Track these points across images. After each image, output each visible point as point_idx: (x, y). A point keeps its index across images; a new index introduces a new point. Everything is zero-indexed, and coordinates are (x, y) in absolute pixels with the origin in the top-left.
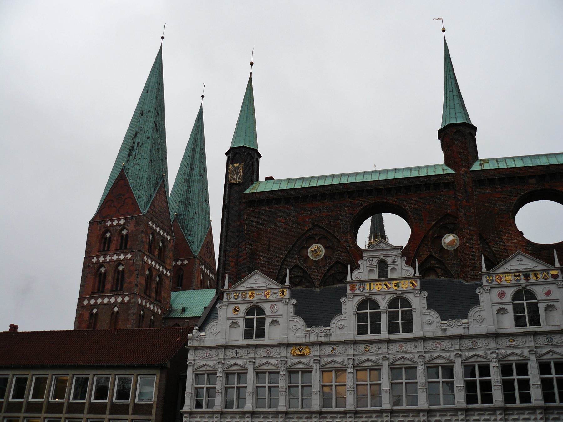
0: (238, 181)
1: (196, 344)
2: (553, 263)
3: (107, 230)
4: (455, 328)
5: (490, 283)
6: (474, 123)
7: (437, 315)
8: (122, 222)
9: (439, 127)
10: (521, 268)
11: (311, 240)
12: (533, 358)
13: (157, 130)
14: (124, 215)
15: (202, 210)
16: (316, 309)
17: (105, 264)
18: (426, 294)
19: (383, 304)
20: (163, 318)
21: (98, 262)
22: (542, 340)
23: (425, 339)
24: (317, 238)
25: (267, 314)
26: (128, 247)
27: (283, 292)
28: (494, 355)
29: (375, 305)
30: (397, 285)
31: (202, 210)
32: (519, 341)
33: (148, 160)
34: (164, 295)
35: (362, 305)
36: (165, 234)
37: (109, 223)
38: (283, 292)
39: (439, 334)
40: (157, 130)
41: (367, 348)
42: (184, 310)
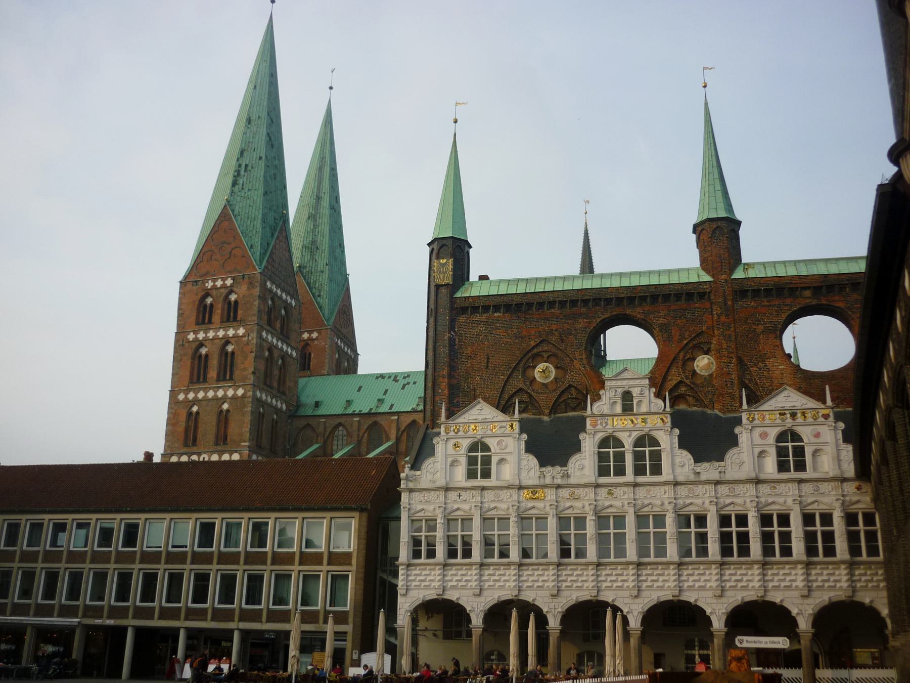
0: (446, 282)
1: (411, 485)
2: (824, 402)
4: (709, 471)
5: (752, 422)
6: (739, 216)
7: (690, 456)
8: (229, 282)
9: (695, 220)
10: (788, 405)
11: (537, 358)
12: (797, 508)
13: (272, 146)
14: (230, 272)
15: (335, 258)
16: (551, 445)
17: (206, 343)
18: (677, 431)
19: (628, 442)
20: (290, 417)
22: (807, 488)
23: (676, 484)
24: (545, 355)
25: (493, 451)
26: (239, 319)
27: (512, 426)
28: (754, 504)
29: (619, 443)
30: (644, 421)
31: (335, 258)
32: (781, 488)
33: (261, 191)
34: (289, 383)
35: (604, 443)
36: (288, 298)
37: (210, 284)
38: (512, 426)
39: (692, 477)
40: (272, 146)
41: (610, 493)
42: (317, 404)
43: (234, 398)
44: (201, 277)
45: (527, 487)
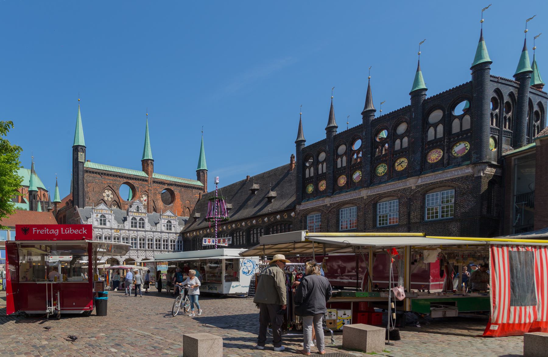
19: (138, 219)
29: (135, 219)
35: (132, 219)
45: (114, 229)
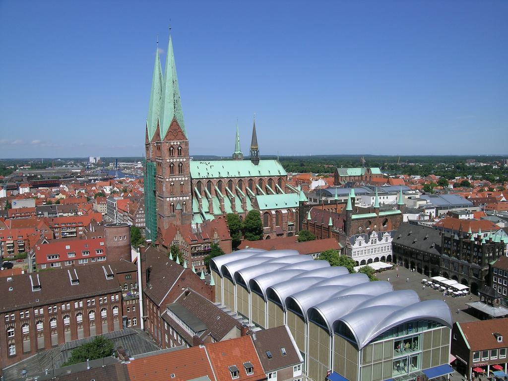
3: (172, 147)
8: (179, 143)
21: (170, 162)
37: (172, 144)
43: (185, 180)
44: (169, 140)
